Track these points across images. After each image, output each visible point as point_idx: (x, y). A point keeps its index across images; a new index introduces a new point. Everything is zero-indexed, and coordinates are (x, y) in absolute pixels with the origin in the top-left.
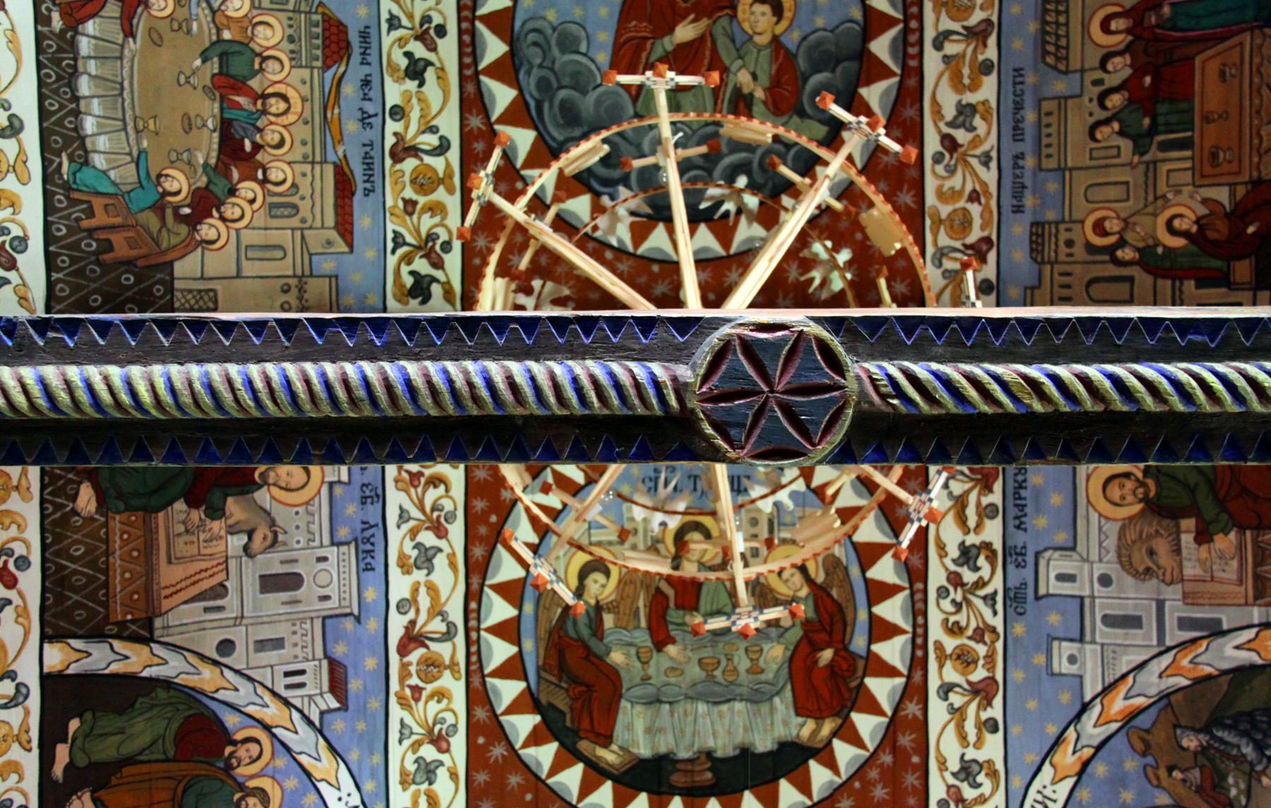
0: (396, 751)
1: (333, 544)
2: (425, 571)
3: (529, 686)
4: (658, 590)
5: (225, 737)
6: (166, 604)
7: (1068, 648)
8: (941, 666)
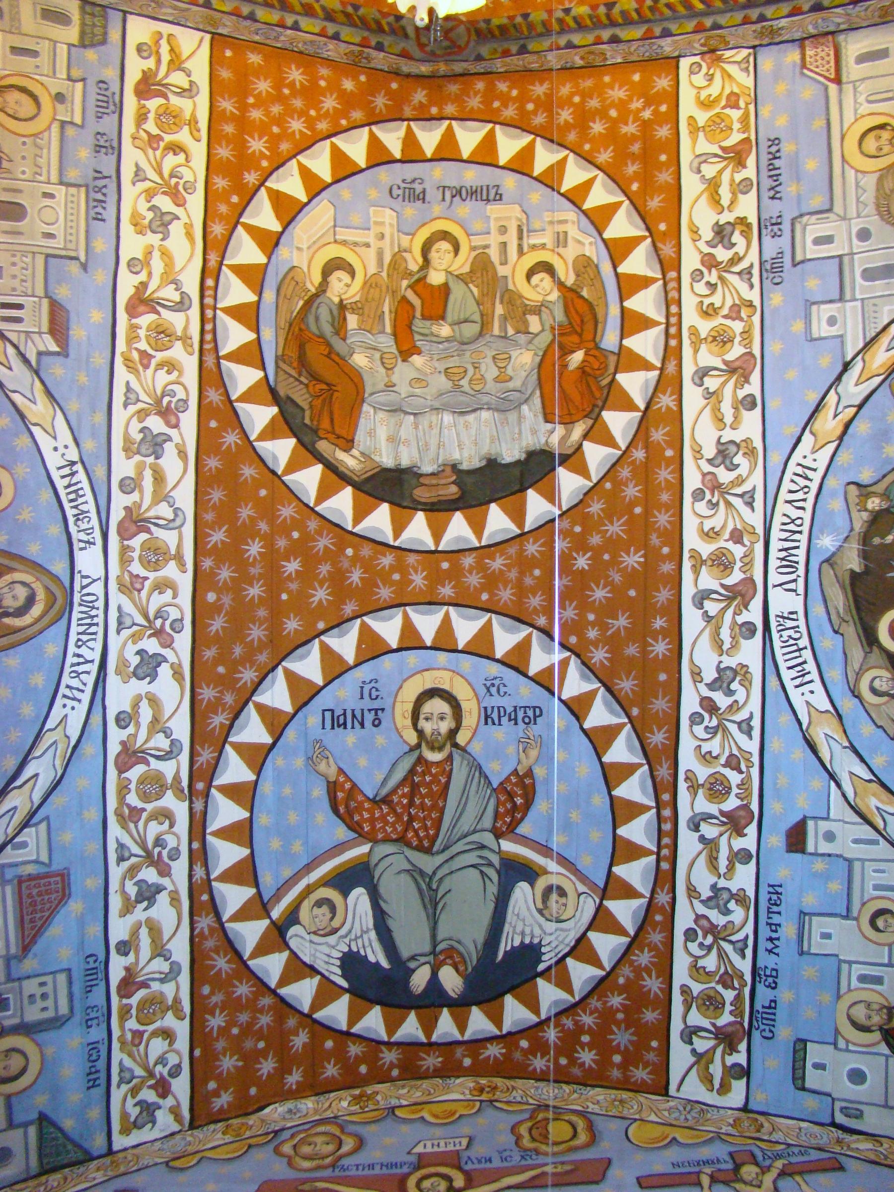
0: (120, 415)
1: (61, 183)
2: (160, 236)
3: (266, 376)
4: (404, 299)
7: (827, 310)
8: (696, 351)
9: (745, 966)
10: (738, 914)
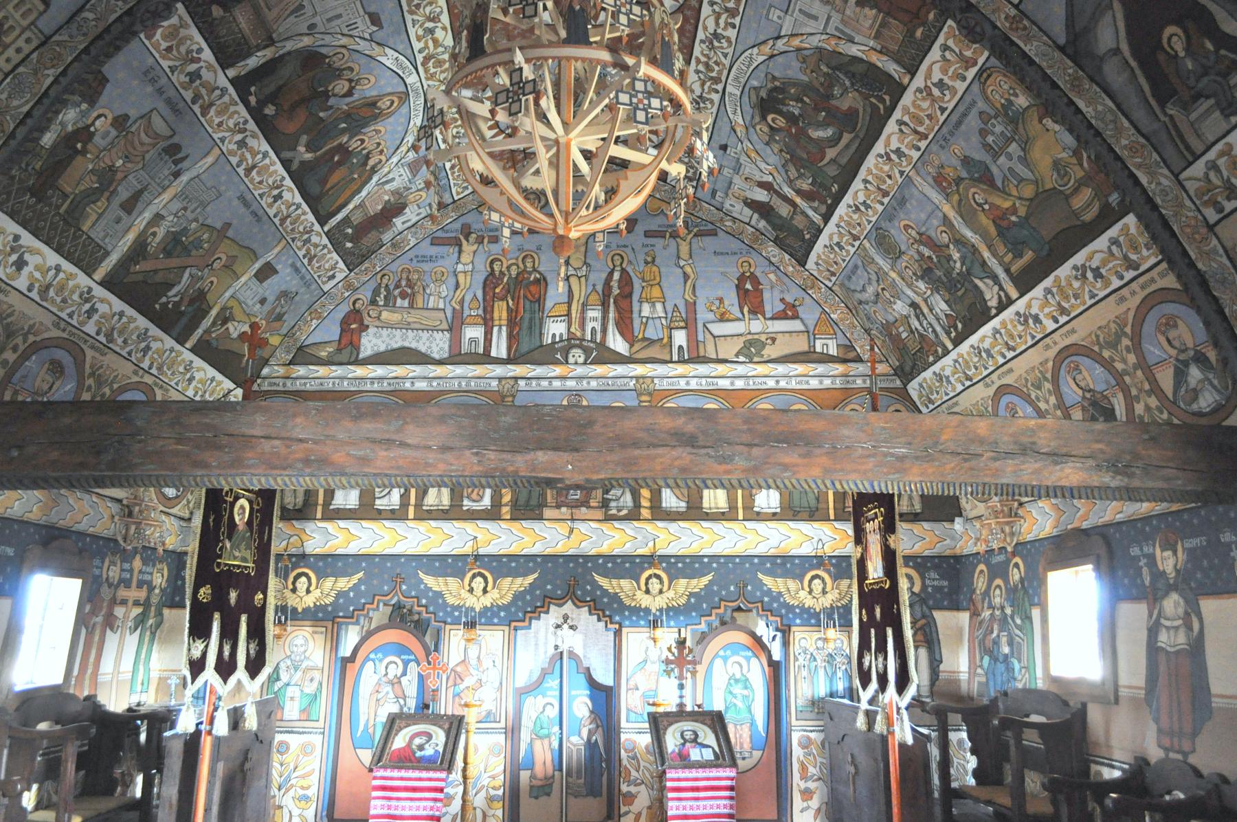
6: (275, 27)
7: (778, 12)
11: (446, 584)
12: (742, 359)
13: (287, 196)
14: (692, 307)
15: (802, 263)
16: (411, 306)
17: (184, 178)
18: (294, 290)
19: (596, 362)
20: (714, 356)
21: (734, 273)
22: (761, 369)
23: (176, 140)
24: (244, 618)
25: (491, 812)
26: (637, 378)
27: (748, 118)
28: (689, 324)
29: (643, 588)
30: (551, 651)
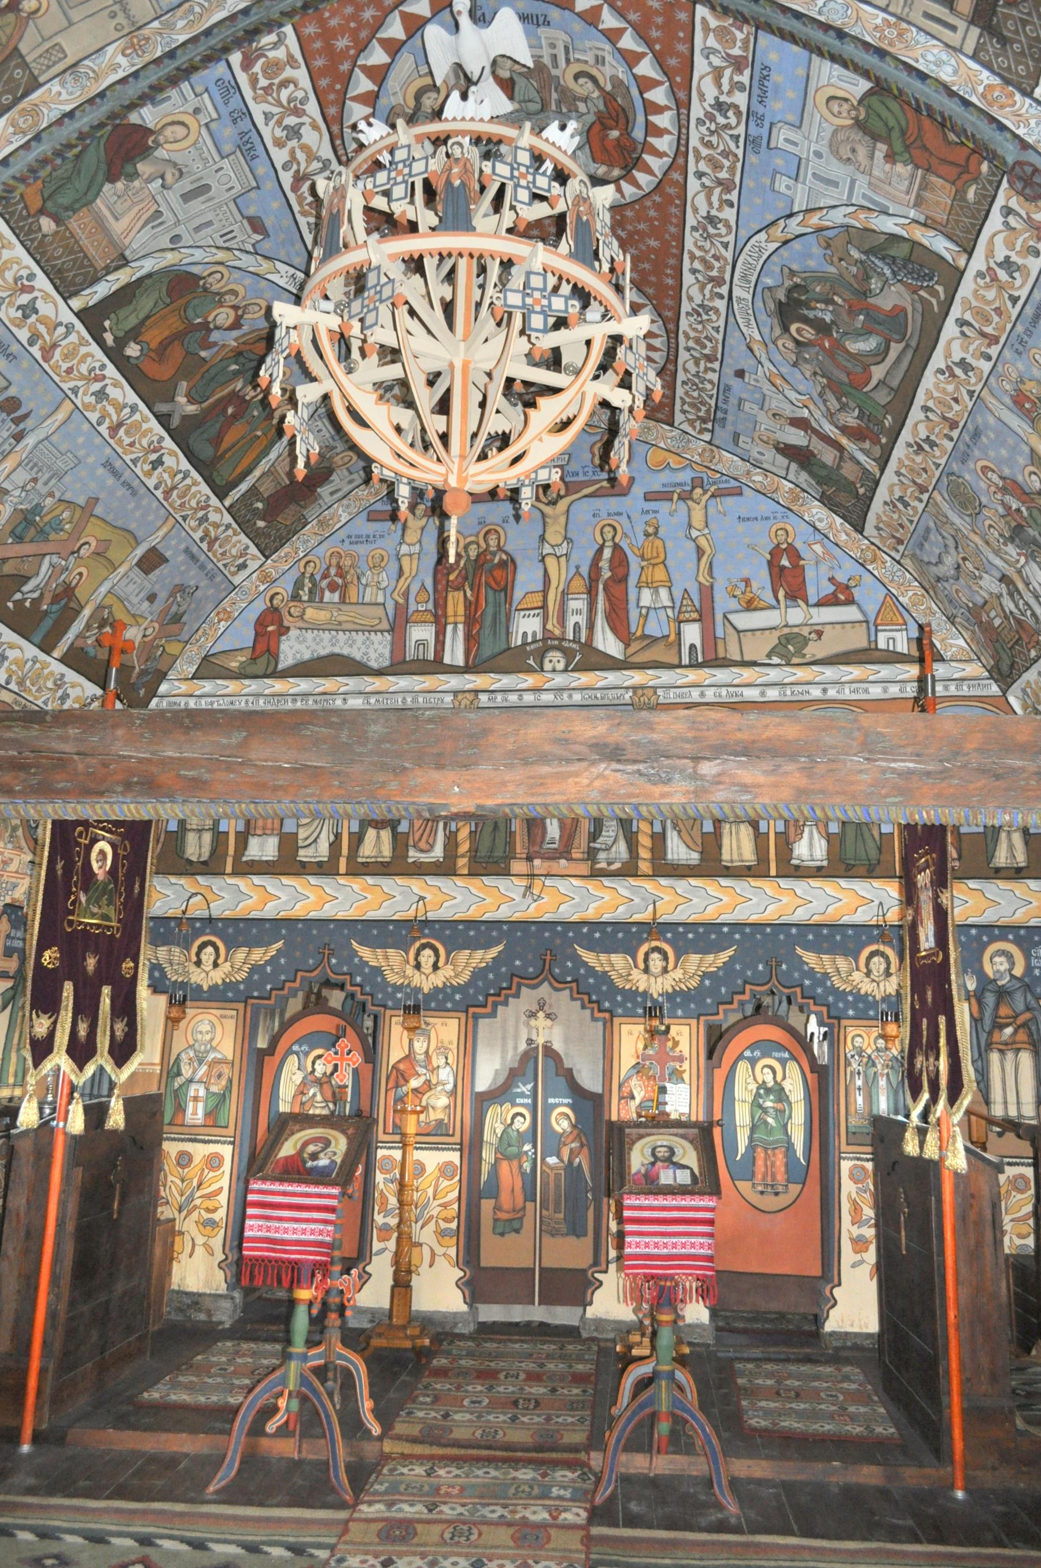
5: (197, 278)
6: (127, 242)
9: (713, 403)
10: (709, 386)
11: (386, 958)
12: (776, 660)
13: (169, 461)
14: (707, 593)
15: (860, 529)
16: (343, 600)
17: (30, 441)
18: (192, 583)
19: (584, 667)
20: (738, 658)
21: (766, 546)
22: (801, 674)
23: (12, 392)
24: (106, 990)
25: (439, 1250)
26: (634, 688)
27: (766, 330)
28: (705, 615)
29: (642, 966)
30: (523, 1046)
